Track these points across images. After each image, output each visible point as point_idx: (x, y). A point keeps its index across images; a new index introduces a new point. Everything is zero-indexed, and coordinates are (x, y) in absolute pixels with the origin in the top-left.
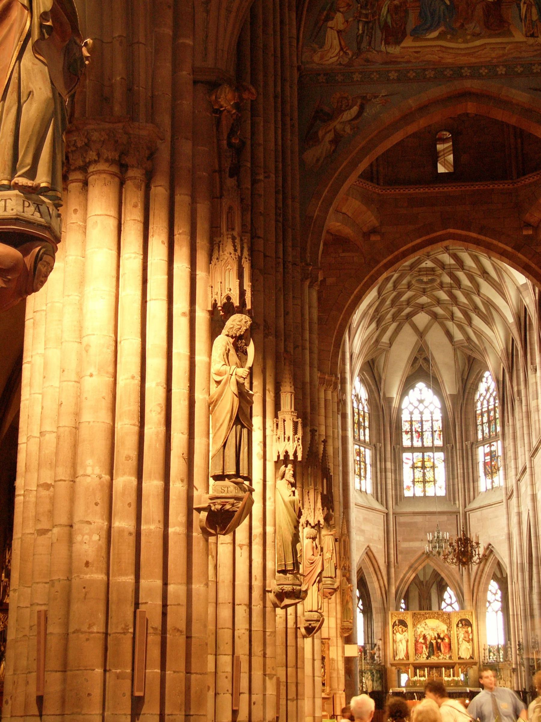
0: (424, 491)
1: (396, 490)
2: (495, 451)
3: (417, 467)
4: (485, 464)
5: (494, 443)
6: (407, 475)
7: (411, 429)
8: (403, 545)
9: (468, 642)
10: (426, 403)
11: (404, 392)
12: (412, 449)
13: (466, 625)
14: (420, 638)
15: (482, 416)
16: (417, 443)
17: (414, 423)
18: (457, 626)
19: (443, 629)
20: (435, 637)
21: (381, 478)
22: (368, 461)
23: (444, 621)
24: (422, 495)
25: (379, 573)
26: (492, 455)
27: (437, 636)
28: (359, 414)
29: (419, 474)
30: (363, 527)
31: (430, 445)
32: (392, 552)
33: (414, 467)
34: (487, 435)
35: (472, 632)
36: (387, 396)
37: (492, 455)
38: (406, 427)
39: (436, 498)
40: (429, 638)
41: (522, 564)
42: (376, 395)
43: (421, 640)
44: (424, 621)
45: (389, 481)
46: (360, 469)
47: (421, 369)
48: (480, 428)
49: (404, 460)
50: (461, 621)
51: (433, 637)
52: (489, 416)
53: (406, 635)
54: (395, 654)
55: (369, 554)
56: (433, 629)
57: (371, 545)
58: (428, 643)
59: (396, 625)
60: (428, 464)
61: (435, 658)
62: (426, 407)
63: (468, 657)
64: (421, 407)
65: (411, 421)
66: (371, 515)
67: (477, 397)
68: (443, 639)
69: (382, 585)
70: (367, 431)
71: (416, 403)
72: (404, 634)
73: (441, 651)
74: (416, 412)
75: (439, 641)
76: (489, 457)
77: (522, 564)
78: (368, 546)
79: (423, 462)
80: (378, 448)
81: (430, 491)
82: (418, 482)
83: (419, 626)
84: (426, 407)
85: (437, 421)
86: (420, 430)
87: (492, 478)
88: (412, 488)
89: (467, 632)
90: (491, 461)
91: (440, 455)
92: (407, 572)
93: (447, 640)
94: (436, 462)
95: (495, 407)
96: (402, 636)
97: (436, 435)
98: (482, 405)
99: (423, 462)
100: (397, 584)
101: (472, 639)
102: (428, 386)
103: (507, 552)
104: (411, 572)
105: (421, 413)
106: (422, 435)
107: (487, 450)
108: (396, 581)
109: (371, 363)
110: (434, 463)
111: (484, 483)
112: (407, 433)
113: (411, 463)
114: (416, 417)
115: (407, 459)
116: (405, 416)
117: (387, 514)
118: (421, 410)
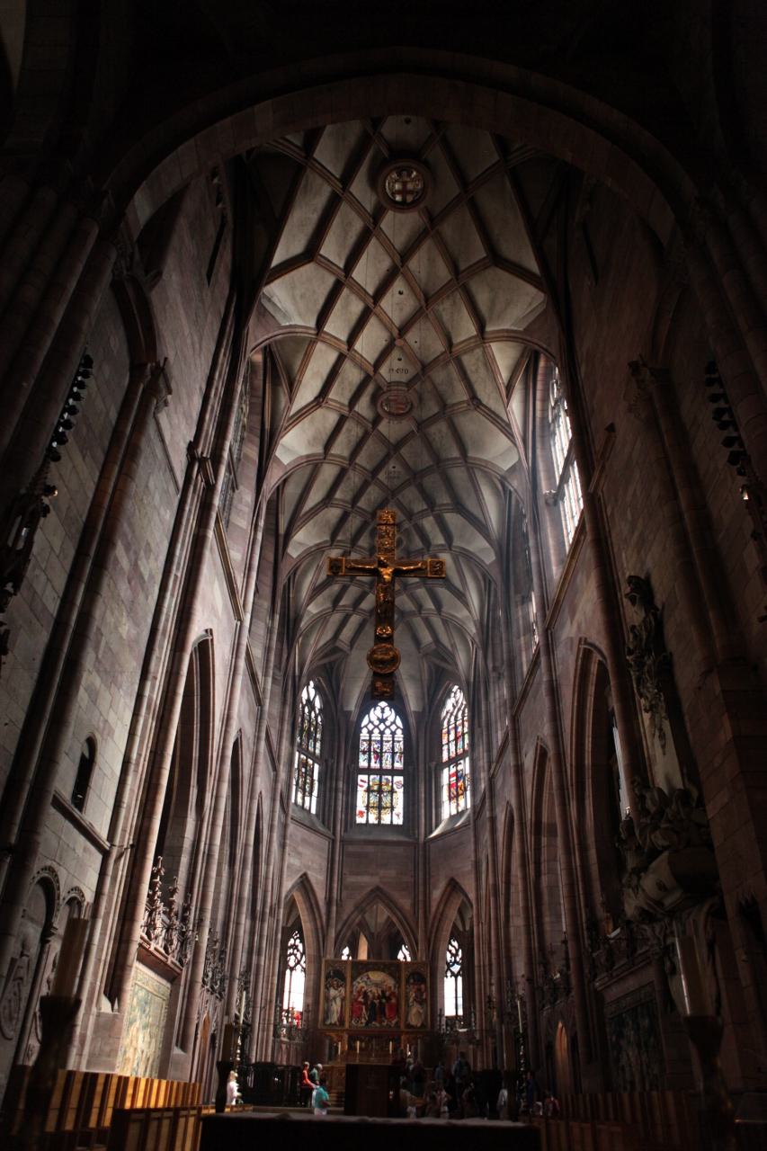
0: (379, 818)
1: (346, 815)
2: (462, 770)
3: (374, 791)
4: (450, 786)
5: (462, 761)
6: (361, 799)
7: (370, 749)
8: (350, 879)
10: (388, 723)
11: (364, 710)
12: (369, 771)
14: (359, 996)
15: (448, 733)
16: (375, 765)
17: (373, 743)
18: (407, 982)
21: (330, 799)
22: (316, 776)
23: (391, 974)
24: (376, 822)
25: (315, 910)
26: (458, 776)
28: (309, 721)
29: (374, 799)
30: (300, 849)
31: (389, 767)
32: (335, 885)
33: (369, 790)
34: (453, 755)
35: (426, 990)
36: (345, 709)
37: (458, 776)
38: (364, 746)
39: (392, 827)
40: (370, 995)
41: (495, 886)
42: (333, 706)
43: (361, 999)
45: (340, 803)
46: (305, 783)
47: (384, 688)
48: (445, 748)
49: (359, 782)
53: (343, 992)
54: (327, 1013)
55: (304, 883)
57: (309, 873)
58: (369, 1003)
60: (385, 788)
61: (378, 1025)
63: (419, 1025)
64: (382, 727)
65: (370, 741)
66: (313, 838)
67: (444, 714)
70: (318, 745)
71: (377, 723)
73: (385, 1015)
74: (376, 731)
76: (455, 778)
77: (495, 886)
79: (380, 785)
80: (330, 764)
81: (386, 819)
82: (373, 807)
83: (359, 980)
85: (399, 742)
86: (378, 751)
87: (457, 800)
88: (365, 815)
89: (419, 990)
90: (457, 783)
91: (399, 779)
92: (352, 913)
93: (394, 1001)
94: (395, 786)
95: (463, 721)
97: (397, 758)
98: (449, 722)
99: (380, 785)
100: (339, 927)
102: (391, 706)
103: (473, 885)
104: (356, 913)
105: (382, 733)
106: (382, 756)
107: (453, 770)
108: (337, 921)
109: (328, 666)
110: (392, 786)
112: (364, 753)
113: (366, 785)
114: (376, 736)
115: (362, 781)
116: (364, 735)
117: (334, 841)
118: (382, 729)
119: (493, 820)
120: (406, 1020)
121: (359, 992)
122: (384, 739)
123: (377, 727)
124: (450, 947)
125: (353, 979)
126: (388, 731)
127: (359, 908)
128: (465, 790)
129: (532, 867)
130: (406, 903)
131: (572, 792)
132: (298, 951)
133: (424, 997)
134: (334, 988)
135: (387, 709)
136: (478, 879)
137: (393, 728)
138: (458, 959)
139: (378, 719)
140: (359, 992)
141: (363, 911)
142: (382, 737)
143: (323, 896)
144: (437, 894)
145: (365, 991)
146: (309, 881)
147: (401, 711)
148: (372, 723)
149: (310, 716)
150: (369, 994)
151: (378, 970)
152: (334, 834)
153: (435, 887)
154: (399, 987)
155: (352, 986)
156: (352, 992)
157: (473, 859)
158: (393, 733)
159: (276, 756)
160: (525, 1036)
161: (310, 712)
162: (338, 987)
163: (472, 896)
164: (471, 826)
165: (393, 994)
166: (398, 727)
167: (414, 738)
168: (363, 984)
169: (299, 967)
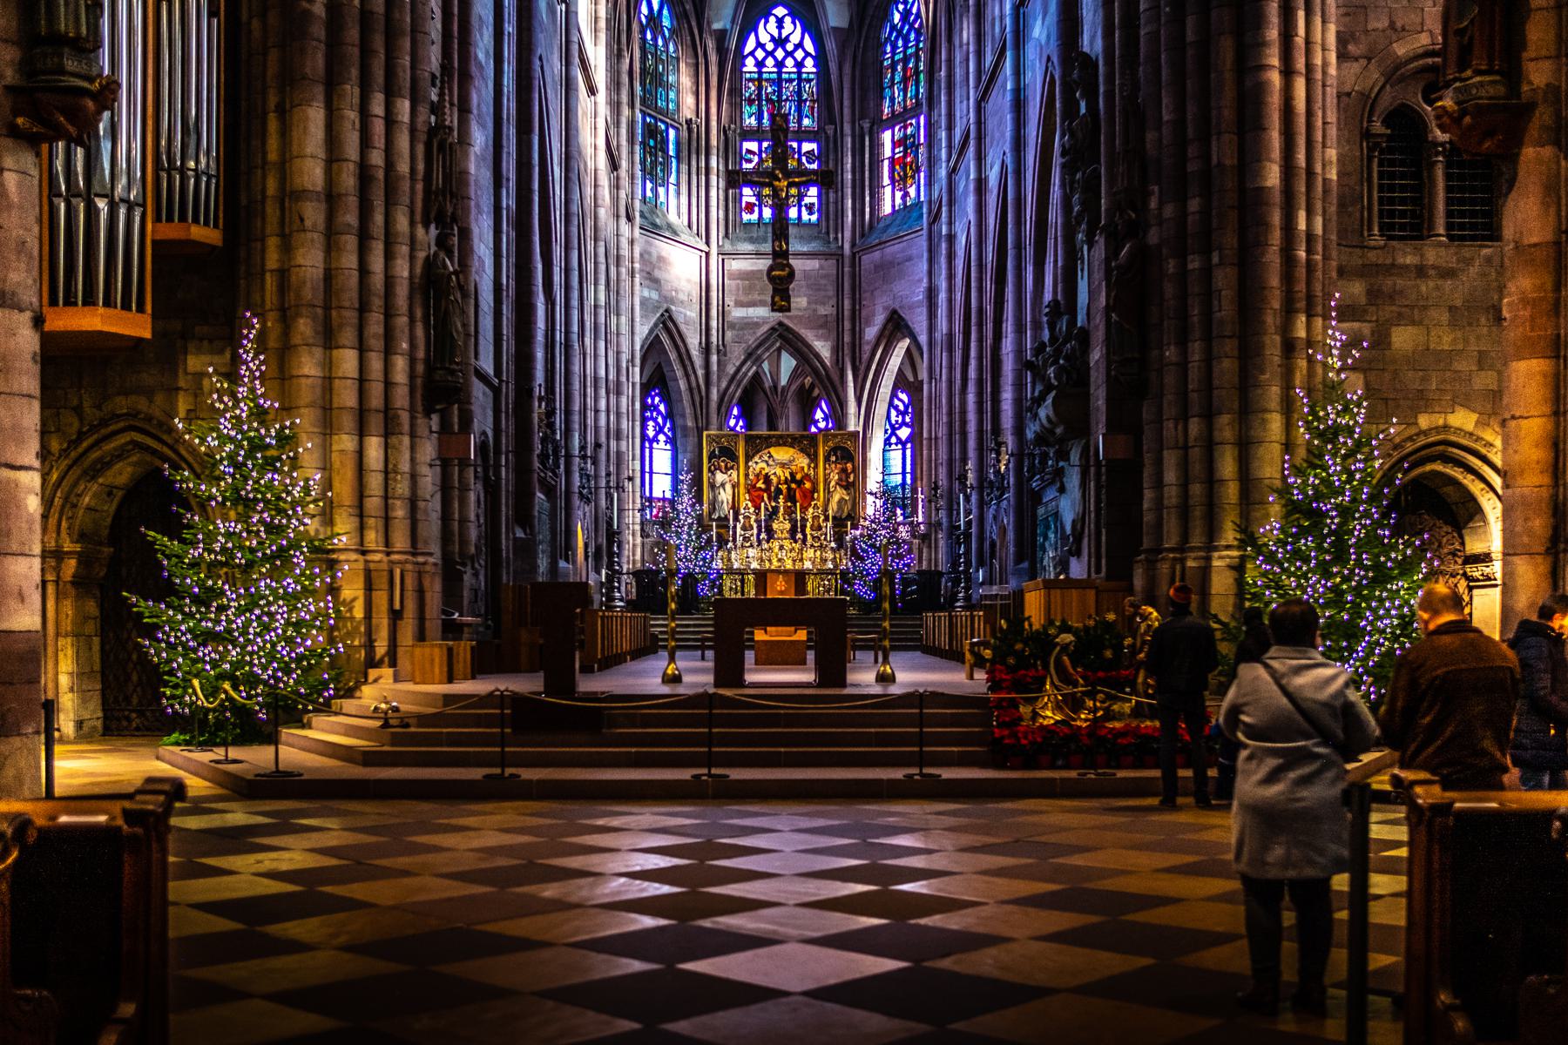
4: (892, 161)
9: (846, 488)
10: (790, 47)
11: (749, 27)
13: (843, 458)
15: (893, 67)
18: (827, 459)
23: (802, 450)
40: (775, 480)
43: (760, 485)
50: (834, 450)
52: (905, 69)
56: (783, 465)
62: (789, 54)
65: (760, 79)
68: (800, 483)
69: (694, 384)
71: (770, 47)
74: (770, 62)
78: (667, 311)
83: (756, 459)
84: (789, 54)
89: (844, 470)
93: (808, 485)
95: (918, 50)
97: (806, 110)
98: (894, 47)
100: (724, 385)
101: (853, 484)
103: (925, 324)
105: (780, 65)
111: (889, 200)
112: (750, 102)
117: (707, 254)
119: (951, 238)
121: (757, 476)
122: (785, 76)
123: (771, 54)
124: (896, 402)
125: (748, 458)
126: (790, 62)
127: (751, 355)
128: (918, 170)
129: (990, 326)
130: (823, 349)
131: (1029, 252)
132: (659, 413)
135: (788, 20)
136: (932, 315)
137: (799, 55)
138: (908, 419)
139: (773, 39)
140: (757, 476)
141: (758, 361)
142: (780, 73)
143: (696, 342)
144: (871, 333)
146: (670, 317)
147: (811, 26)
148: (762, 46)
149: (656, 45)
151: (785, 444)
152: (708, 243)
153: (869, 323)
154: (816, 467)
155: (747, 467)
156: (747, 475)
157: (925, 283)
158: (799, 65)
159: (615, 153)
160: (968, 535)
161: (655, 39)
162: (727, 469)
163: (923, 339)
164: (925, 232)
165: (807, 477)
166: (807, 54)
167: (834, 77)
169: (662, 437)
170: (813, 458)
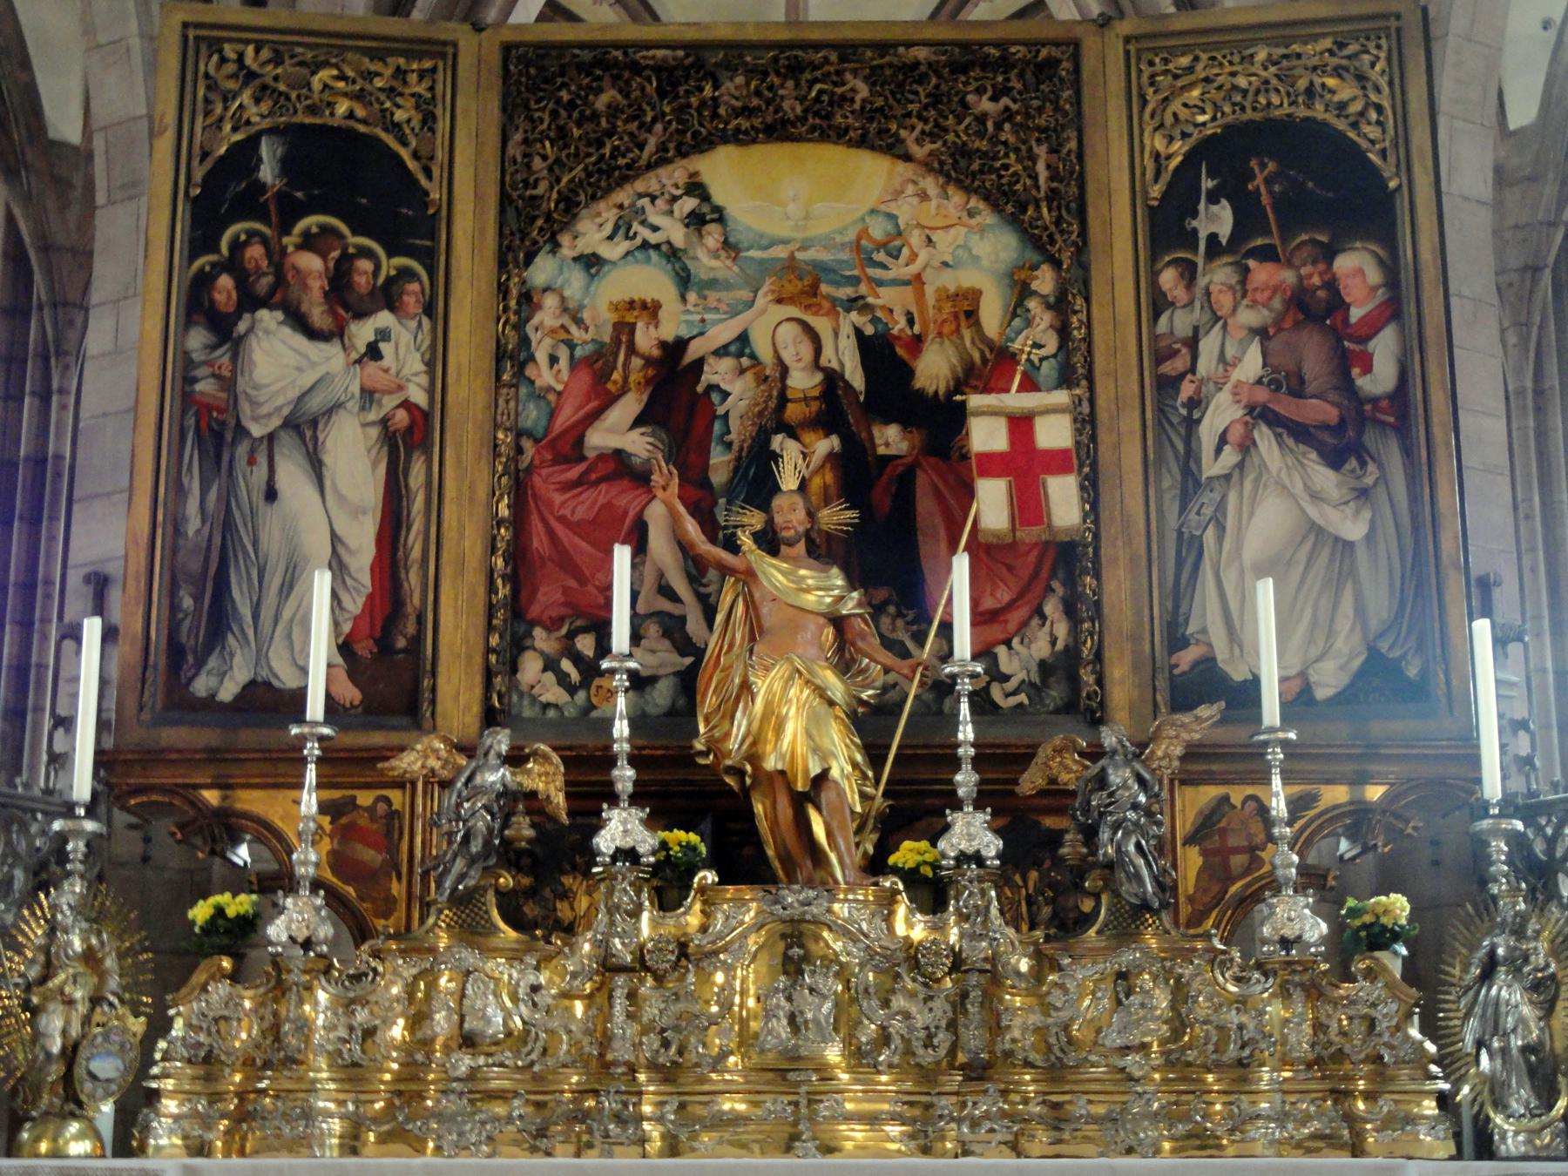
9: (1340, 446)
13: (1295, 211)
18: (1167, 228)
19: (968, 278)
20: (833, 380)
23: (962, 169)
27: (857, 379)
40: (738, 395)
43: (618, 431)
44: (674, 175)
50: (1224, 156)
51: (802, 381)
53: (405, 353)
59: (251, 202)
72: (362, 332)
75: (891, 439)
83: (592, 231)
89: (1316, 309)
96: (330, 357)
120: (1176, 641)
125: (527, 225)
133: (1380, 378)
134: (299, 322)
145: (681, 345)
150: (718, 372)
156: (511, 358)
162: (346, 299)
168: (649, 281)
170: (1052, 225)
